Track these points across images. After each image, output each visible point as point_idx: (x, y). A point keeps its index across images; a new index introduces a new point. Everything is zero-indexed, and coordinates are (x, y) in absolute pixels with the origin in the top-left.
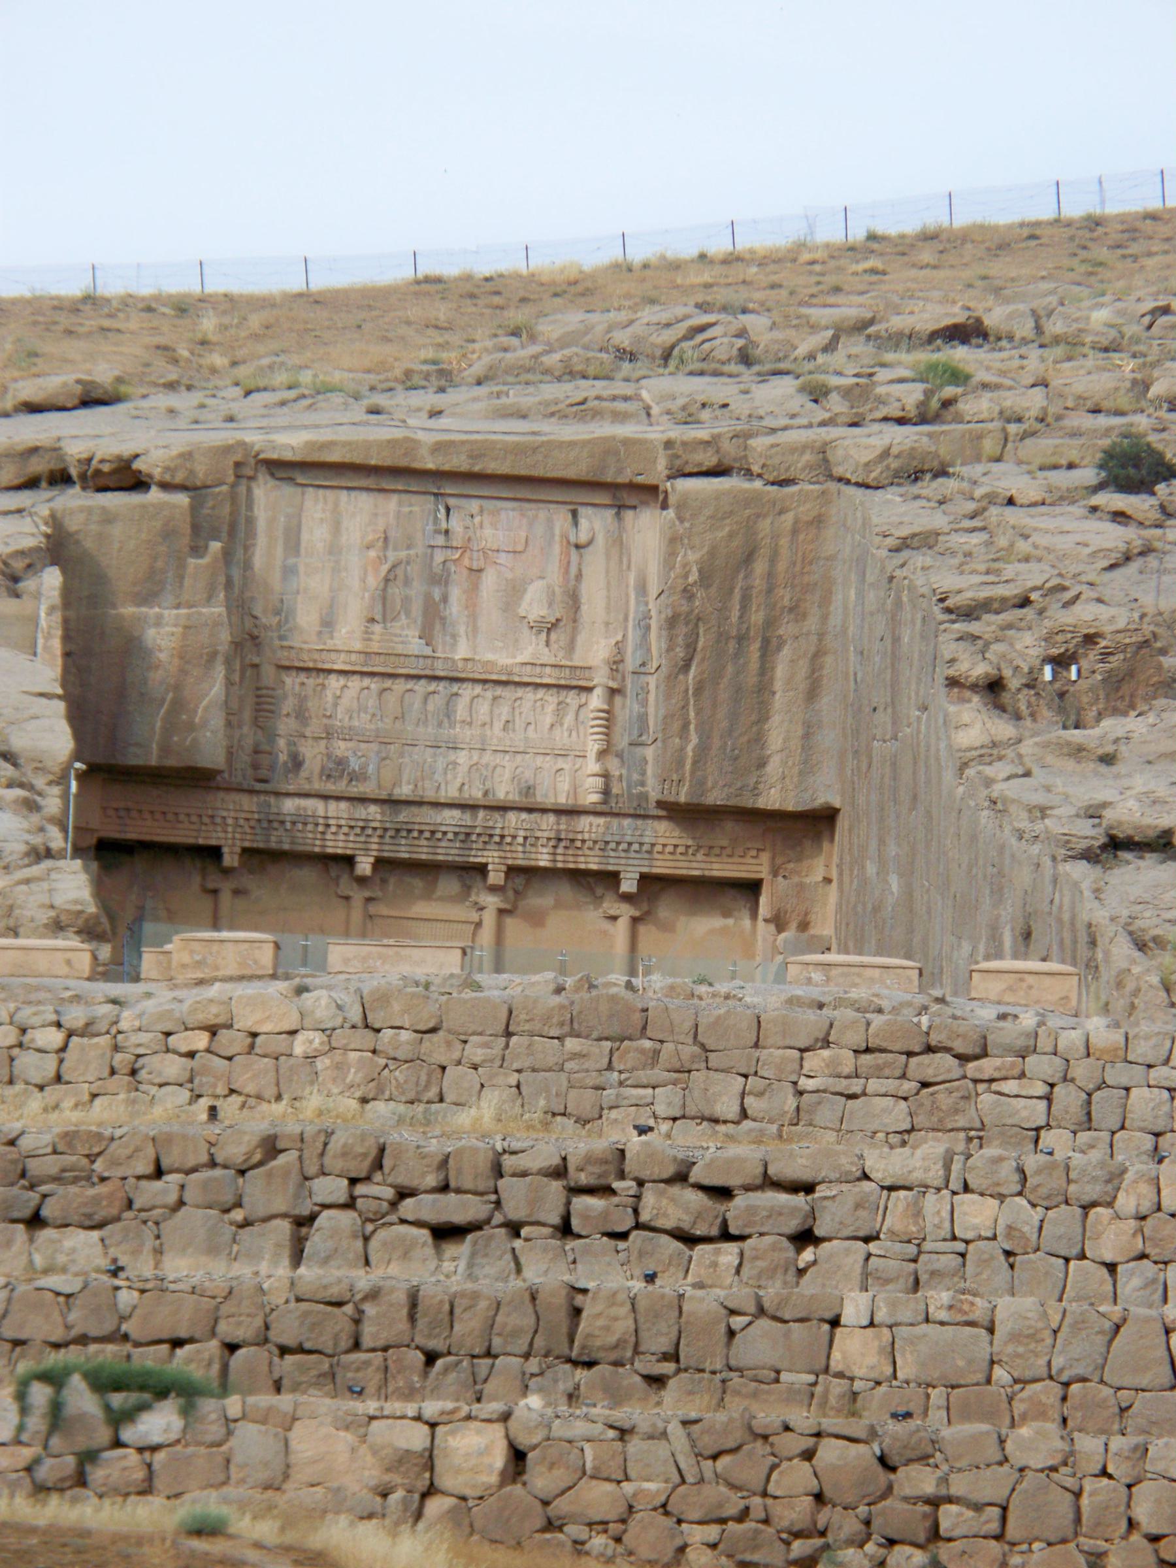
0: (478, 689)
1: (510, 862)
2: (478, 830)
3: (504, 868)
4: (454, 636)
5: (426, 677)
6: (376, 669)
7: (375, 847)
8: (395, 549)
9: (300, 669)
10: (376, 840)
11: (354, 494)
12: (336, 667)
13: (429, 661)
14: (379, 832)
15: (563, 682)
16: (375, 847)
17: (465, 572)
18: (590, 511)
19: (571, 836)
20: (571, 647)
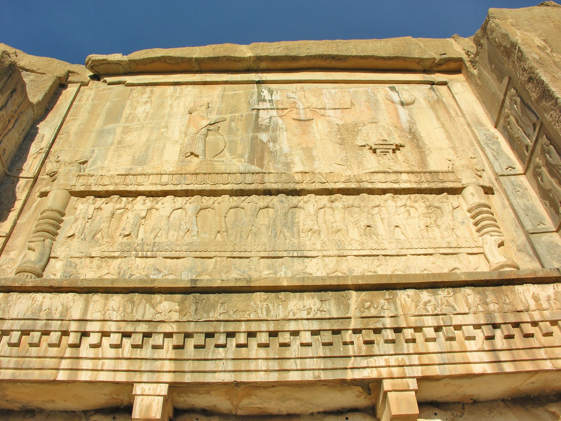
0: (325, 199)
1: (418, 372)
2: (353, 324)
3: (413, 384)
4: (288, 165)
5: (257, 192)
6: (190, 187)
7: (168, 366)
8: (217, 114)
9: (98, 195)
10: (171, 354)
11: (178, 88)
12: (141, 188)
13: (256, 177)
14: (175, 340)
15: (425, 186)
16: (168, 366)
17: (295, 123)
18: (406, 86)
19: (512, 319)
20: (423, 161)
